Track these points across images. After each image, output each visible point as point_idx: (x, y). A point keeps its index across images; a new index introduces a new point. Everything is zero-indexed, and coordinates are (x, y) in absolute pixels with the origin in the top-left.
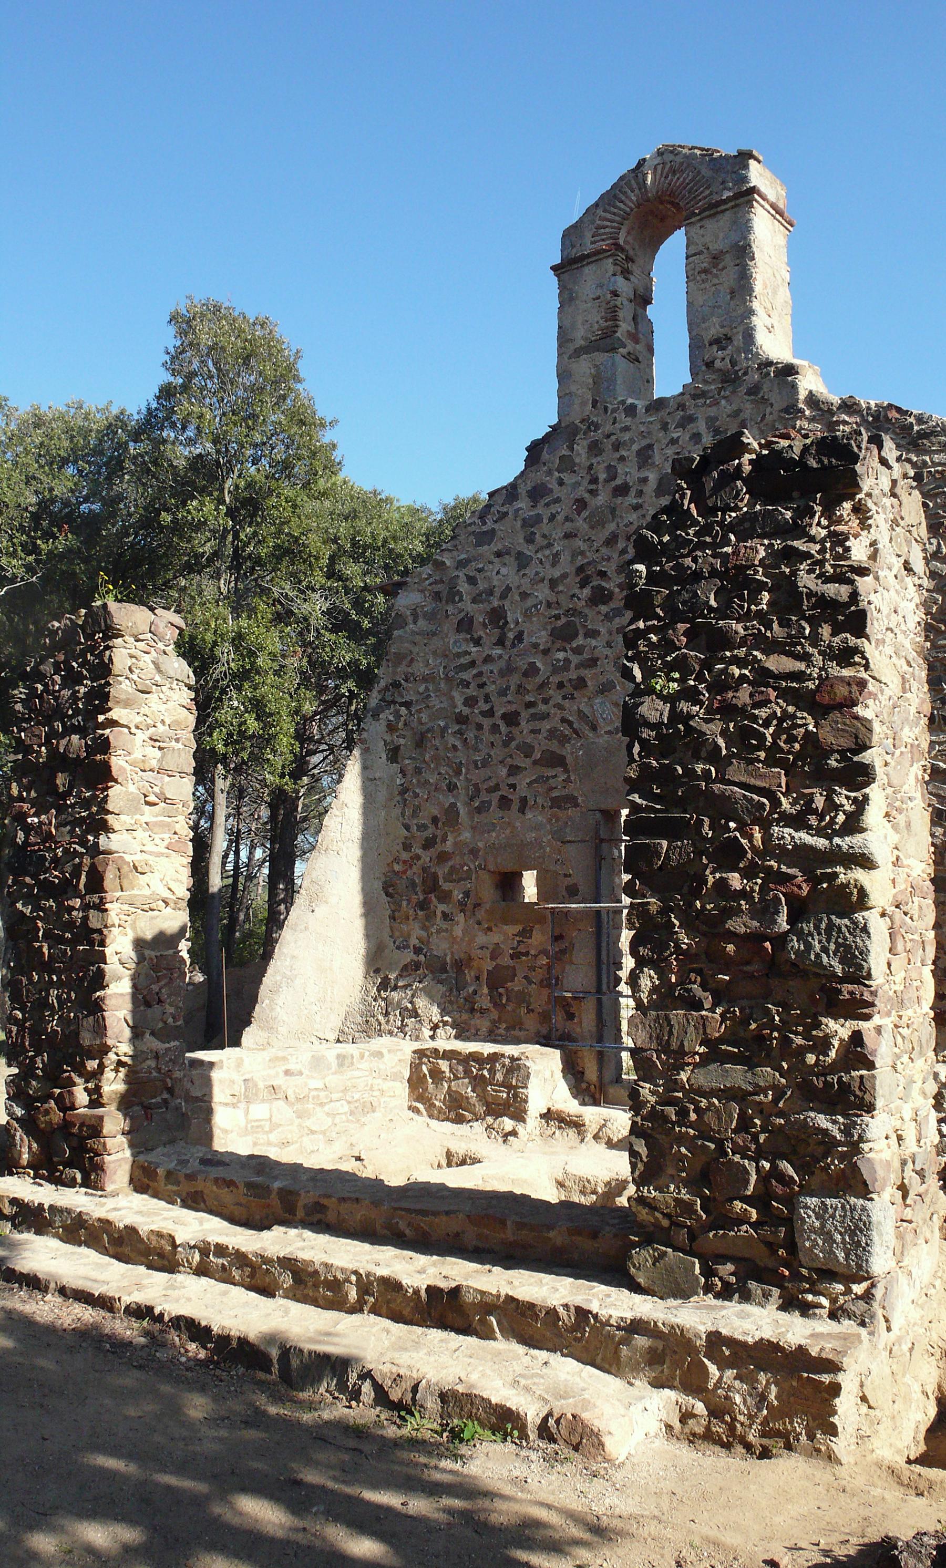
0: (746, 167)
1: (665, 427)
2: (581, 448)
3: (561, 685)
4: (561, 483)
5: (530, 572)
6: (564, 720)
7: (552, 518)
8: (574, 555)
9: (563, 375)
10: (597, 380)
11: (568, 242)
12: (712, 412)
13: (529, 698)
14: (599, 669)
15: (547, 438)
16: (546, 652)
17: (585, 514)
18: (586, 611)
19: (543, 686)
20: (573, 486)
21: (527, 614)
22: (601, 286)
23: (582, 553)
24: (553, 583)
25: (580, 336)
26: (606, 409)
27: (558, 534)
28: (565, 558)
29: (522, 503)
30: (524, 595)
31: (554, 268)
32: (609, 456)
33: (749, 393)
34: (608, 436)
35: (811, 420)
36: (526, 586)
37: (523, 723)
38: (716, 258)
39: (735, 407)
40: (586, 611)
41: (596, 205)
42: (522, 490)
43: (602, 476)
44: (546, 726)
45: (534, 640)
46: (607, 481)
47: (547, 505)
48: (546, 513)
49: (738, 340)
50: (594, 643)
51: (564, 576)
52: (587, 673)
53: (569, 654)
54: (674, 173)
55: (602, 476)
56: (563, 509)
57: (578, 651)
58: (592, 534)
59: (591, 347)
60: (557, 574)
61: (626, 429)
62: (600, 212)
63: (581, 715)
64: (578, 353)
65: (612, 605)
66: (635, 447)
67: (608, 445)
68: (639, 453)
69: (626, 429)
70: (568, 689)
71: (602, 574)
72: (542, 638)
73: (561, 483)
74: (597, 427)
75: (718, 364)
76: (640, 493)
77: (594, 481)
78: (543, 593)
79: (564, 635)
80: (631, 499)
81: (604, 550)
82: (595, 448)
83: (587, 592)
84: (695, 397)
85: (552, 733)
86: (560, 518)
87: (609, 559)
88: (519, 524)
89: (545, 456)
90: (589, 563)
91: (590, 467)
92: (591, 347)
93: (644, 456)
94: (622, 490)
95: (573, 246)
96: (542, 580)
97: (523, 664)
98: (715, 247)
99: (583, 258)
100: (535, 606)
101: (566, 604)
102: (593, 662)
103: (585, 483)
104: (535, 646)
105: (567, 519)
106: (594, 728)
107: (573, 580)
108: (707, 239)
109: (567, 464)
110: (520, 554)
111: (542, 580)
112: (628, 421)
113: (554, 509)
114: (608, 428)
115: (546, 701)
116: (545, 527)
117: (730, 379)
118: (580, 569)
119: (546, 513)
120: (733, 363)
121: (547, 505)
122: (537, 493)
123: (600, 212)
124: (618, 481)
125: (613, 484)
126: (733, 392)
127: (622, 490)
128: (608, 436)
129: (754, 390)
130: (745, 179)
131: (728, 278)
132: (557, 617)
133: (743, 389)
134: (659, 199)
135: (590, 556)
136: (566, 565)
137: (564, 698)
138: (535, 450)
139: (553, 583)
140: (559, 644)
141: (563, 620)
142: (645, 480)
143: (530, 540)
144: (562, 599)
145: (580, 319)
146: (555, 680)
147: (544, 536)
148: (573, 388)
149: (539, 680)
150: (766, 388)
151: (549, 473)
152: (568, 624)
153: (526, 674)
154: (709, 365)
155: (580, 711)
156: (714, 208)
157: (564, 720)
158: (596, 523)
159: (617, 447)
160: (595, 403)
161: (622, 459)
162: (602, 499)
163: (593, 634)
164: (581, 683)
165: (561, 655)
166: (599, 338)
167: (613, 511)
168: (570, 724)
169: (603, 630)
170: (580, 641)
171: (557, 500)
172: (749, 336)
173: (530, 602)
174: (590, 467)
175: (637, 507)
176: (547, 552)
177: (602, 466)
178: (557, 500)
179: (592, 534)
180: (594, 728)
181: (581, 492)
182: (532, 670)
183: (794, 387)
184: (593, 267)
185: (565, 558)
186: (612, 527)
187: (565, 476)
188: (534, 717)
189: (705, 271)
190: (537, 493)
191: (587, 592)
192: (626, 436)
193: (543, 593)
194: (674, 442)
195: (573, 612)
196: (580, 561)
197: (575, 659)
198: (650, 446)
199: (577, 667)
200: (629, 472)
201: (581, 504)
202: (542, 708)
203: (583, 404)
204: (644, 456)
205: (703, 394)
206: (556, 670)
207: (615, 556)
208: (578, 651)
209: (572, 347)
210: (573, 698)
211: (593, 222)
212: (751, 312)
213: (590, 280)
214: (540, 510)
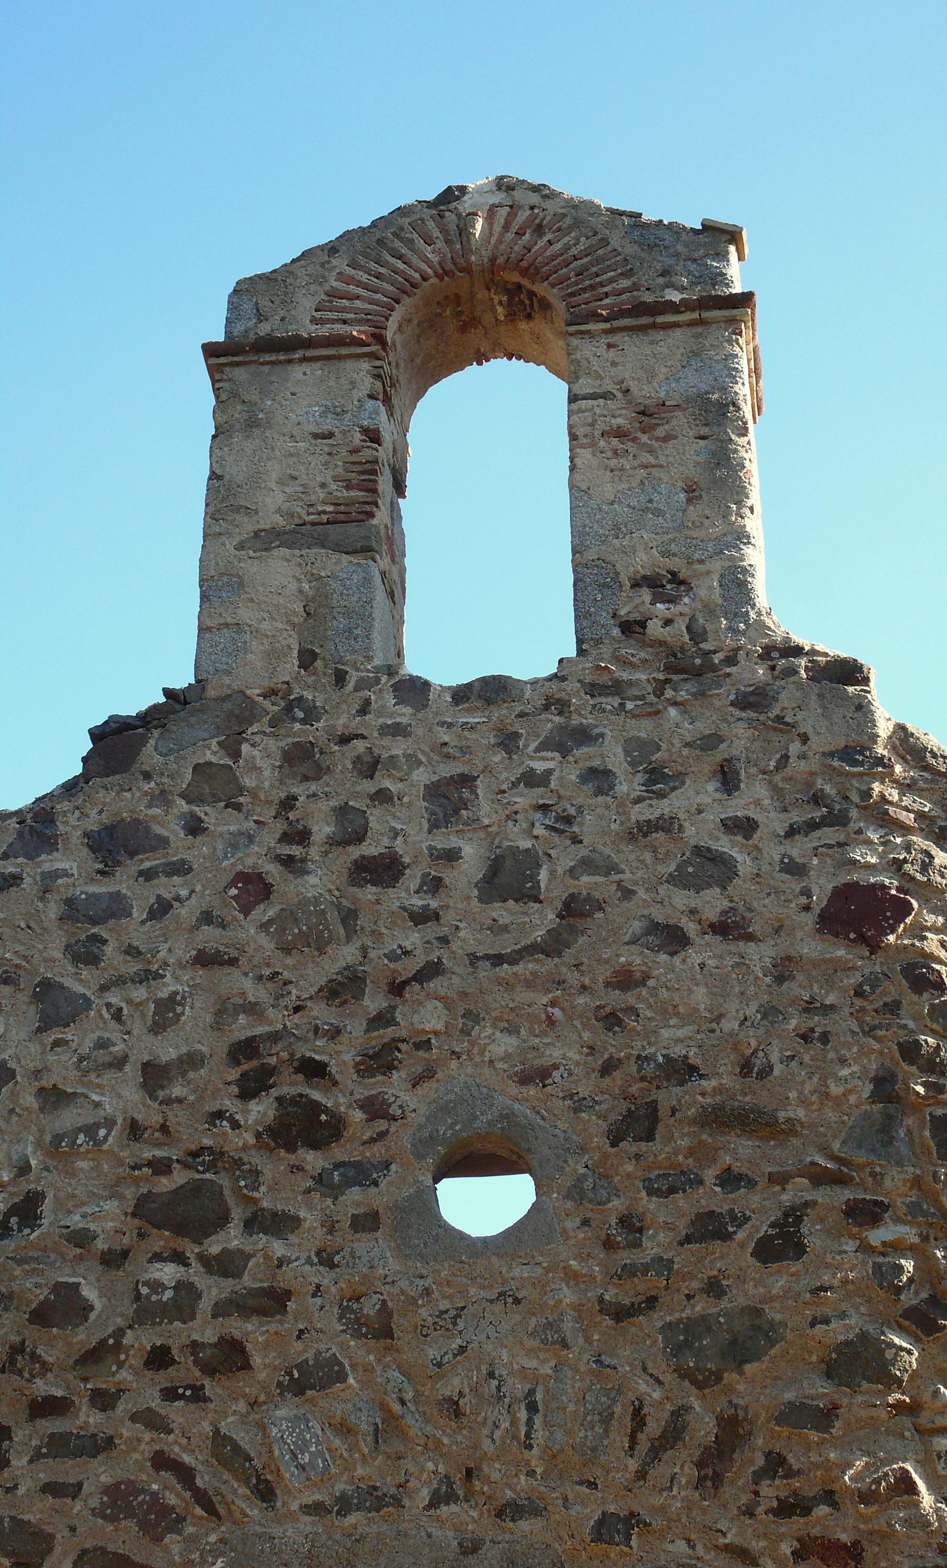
0: (723, 256)
1: (508, 742)
2: (261, 759)
3: (159, 1358)
4: (195, 828)
5: (83, 1037)
6: (161, 1461)
7: (161, 909)
8: (224, 1011)
9: (216, 586)
10: (316, 610)
11: (247, 307)
12: (643, 729)
13: (42, 1387)
14: (288, 1325)
15: (150, 719)
16: (114, 1259)
17: (266, 912)
18: (257, 1159)
19: (94, 1356)
20: (237, 840)
21: (58, 1148)
22: (339, 413)
23: (252, 1009)
24: (154, 1076)
25: (273, 505)
26: (340, 678)
27: (175, 950)
28: (195, 1015)
29: (70, 862)
30: (54, 1098)
31: (210, 350)
32: (343, 784)
33: (742, 703)
34: (345, 740)
35: (906, 787)
36: (62, 1070)
37: (19, 1462)
38: (649, 415)
39: (704, 727)
40: (257, 1159)
41: (332, 249)
42: (71, 826)
43: (322, 829)
44: (99, 1474)
45: (75, 1220)
46: (334, 842)
47: (148, 875)
48: (141, 899)
49: (710, 588)
50: (278, 1248)
51: (192, 1061)
52: (253, 1331)
53: (196, 1274)
54: (539, 230)
55: (322, 829)
56: (194, 896)
57: (226, 1265)
58: (285, 965)
59: (298, 535)
60: (167, 1050)
61: (398, 730)
62: (340, 263)
63: (225, 1450)
64: (265, 540)
65: (340, 1152)
66: (422, 776)
67: (343, 759)
68: (434, 791)
69: (398, 730)
70: (186, 1371)
71: (314, 1070)
72: (108, 1219)
73: (195, 828)
74: (311, 714)
75: (655, 628)
76: (435, 885)
77: (302, 837)
78: (120, 1097)
79: (181, 1216)
80: (406, 894)
81: (320, 1012)
82: (302, 760)
83: (260, 1110)
84: (593, 689)
85: (119, 1500)
86: (186, 913)
87: (335, 1033)
88: (53, 910)
89: (151, 754)
90: (275, 1037)
91: (289, 803)
92: (298, 535)
93: (449, 800)
94: (384, 870)
95: (261, 317)
96: (120, 1063)
97: (35, 1289)
98: (644, 392)
99: (309, 343)
100: (90, 1130)
101: (192, 1133)
102: (273, 1301)
103: (269, 838)
104: (81, 1239)
105: (207, 918)
106: (265, 1492)
107: (218, 1080)
108: (626, 372)
109: (217, 786)
110: (46, 990)
111: (120, 1063)
112: (404, 714)
113: (167, 887)
114: (343, 721)
115: (103, 1400)
116: (135, 929)
117: (689, 665)
118: (244, 1050)
119: (141, 899)
120: (697, 635)
121: (148, 875)
122: (114, 844)
123: (340, 263)
124: (369, 849)
125: (356, 852)
126: (701, 694)
127: (384, 870)
128: (345, 740)
129: (753, 700)
130: (720, 278)
131: (686, 454)
132: (161, 1167)
133: (724, 694)
134: (492, 273)
135: (277, 1019)
136: (194, 1031)
137: (170, 1394)
138: (114, 743)
139: (154, 1076)
140: (160, 1240)
141: (180, 1177)
142: (452, 856)
143: (86, 954)
144: (177, 1117)
145: (274, 471)
146: (141, 1340)
147: (132, 951)
148: (247, 615)
149: (84, 1337)
150: (787, 698)
151: (162, 798)
152: (196, 1188)
153: (41, 1316)
154: (632, 628)
155: (219, 1439)
156: (646, 316)
157: (161, 1461)
158: (302, 935)
159: (369, 767)
160: (307, 659)
161: (382, 797)
162: (319, 882)
163: (279, 1224)
164: (231, 1357)
165: (168, 1273)
166: (308, 527)
167: (349, 917)
168: (185, 1475)
169: (309, 1218)
170: (232, 1238)
171: (181, 869)
172: (737, 584)
173: (69, 1118)
174: (289, 803)
175: (421, 918)
176: (139, 993)
177: (324, 807)
178: (181, 869)
179: (285, 965)
180: (265, 1492)
181: (255, 857)
182: (63, 1307)
183: (862, 708)
184: (315, 370)
185: (195, 1015)
186: (346, 954)
187: (210, 815)
188: (59, 1446)
189: (620, 433)
190: (114, 844)
191: (260, 1110)
192: (398, 748)
193: (120, 1097)
194: (531, 779)
195: (216, 1158)
196: (242, 1028)
197: (213, 1290)
198: (467, 780)
199: (220, 1310)
200: (401, 829)
201: (253, 888)
202: (88, 1418)
203: (274, 655)
204: (449, 800)
205: (617, 688)
206: (146, 1312)
207: (355, 1028)
208: (226, 1265)
209: (248, 526)
210: (198, 1396)
211: (320, 280)
212: (743, 537)
213: (303, 397)
214: (122, 882)
